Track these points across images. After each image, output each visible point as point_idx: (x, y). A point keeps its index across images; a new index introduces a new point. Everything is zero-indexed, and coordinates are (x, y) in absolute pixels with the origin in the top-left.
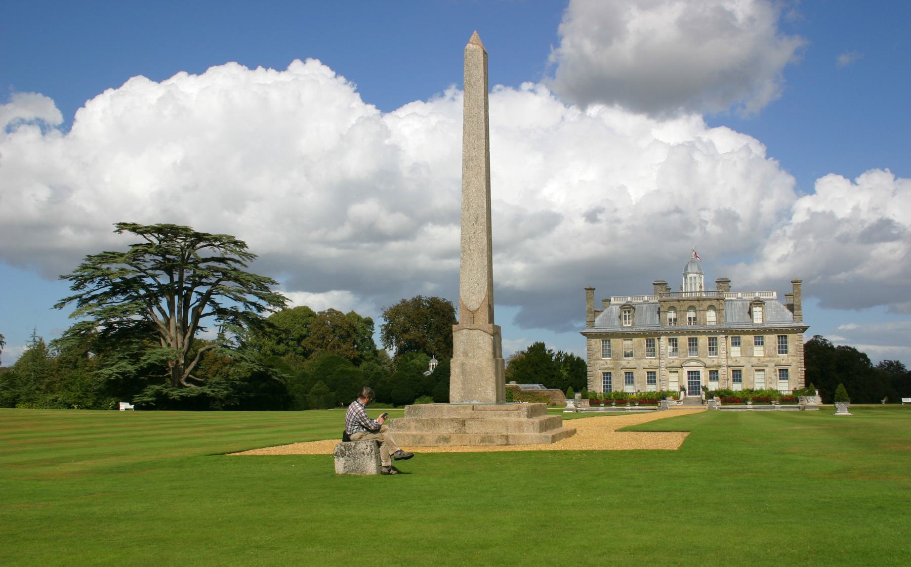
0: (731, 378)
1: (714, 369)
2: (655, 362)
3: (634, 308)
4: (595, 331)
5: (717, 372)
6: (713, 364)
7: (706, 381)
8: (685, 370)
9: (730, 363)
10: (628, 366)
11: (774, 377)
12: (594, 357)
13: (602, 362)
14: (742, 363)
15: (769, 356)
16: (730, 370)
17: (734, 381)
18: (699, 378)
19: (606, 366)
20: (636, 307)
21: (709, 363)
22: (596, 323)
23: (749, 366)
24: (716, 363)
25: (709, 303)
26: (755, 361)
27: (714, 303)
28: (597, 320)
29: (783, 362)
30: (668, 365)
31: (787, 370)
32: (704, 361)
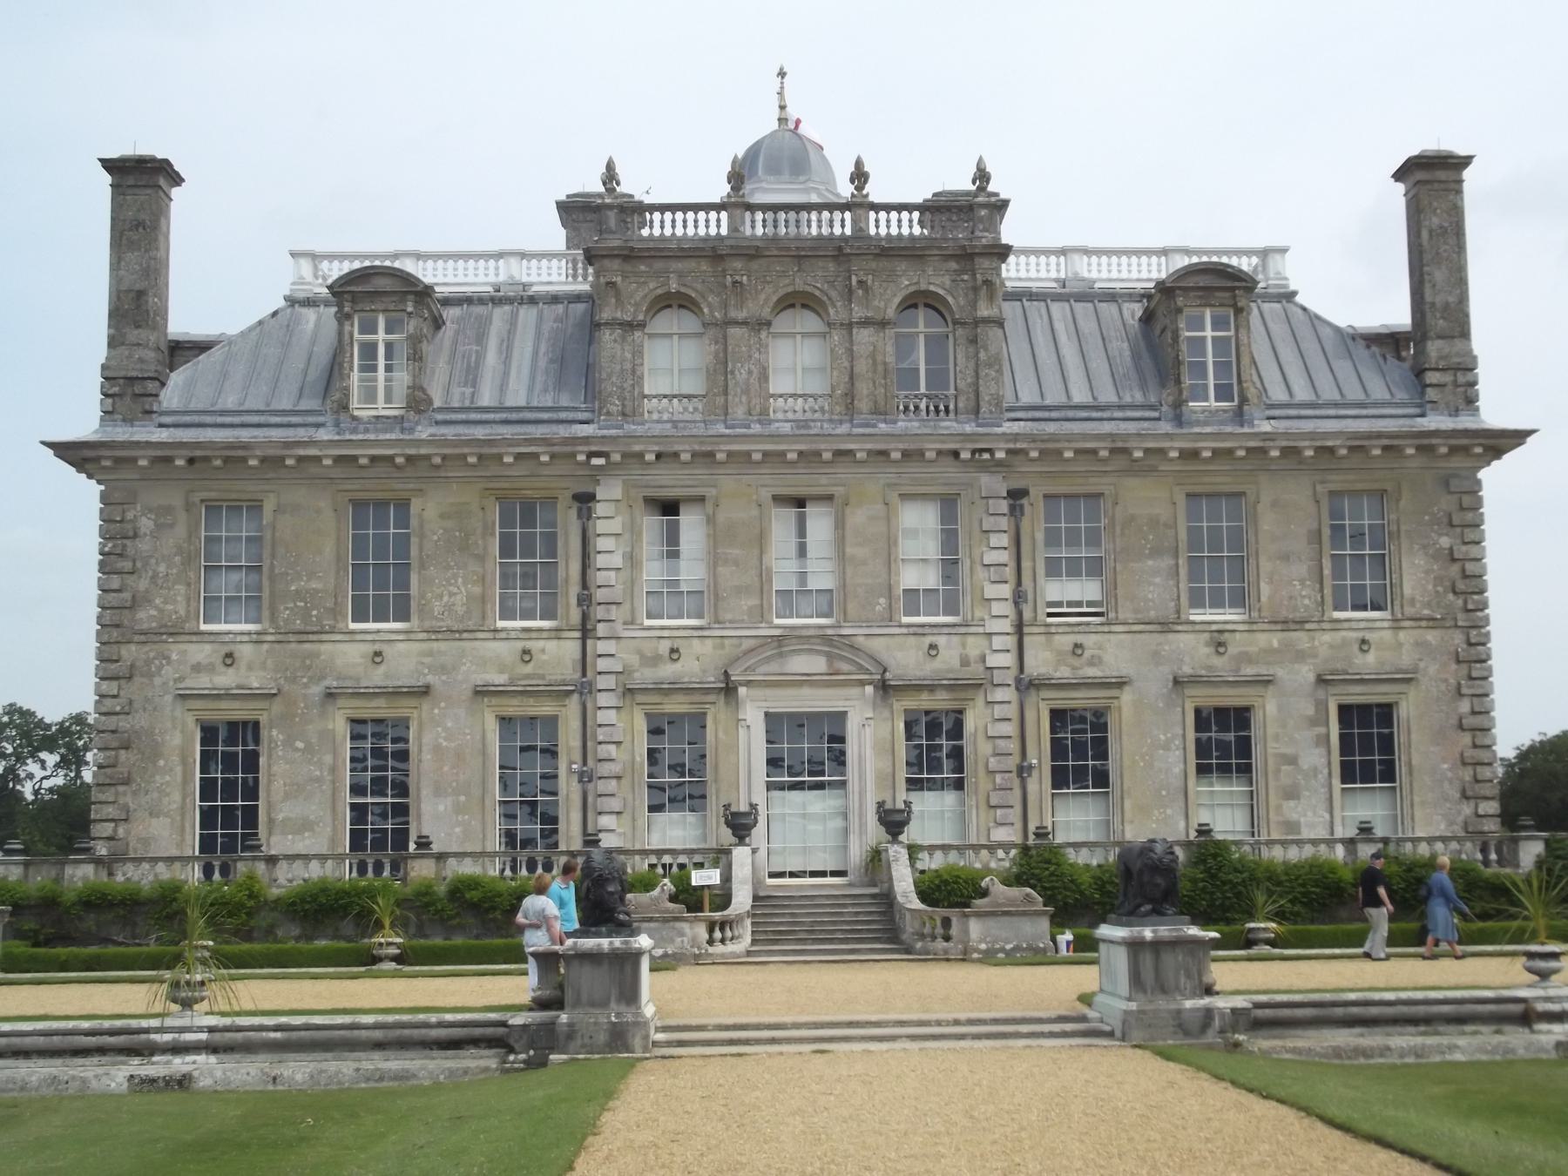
0: (1040, 755)
1: (940, 701)
8: (753, 715)
9: (1040, 661)
10: (377, 677)
12: (146, 617)
13: (201, 653)
15: (1287, 624)
17: (1060, 778)
19: (226, 679)
20: (450, 313)
21: (906, 660)
23: (1153, 683)
24: (949, 657)
25: (908, 280)
26: (1190, 650)
27: (937, 281)
28: (177, 378)
29: (1369, 662)
30: (645, 676)
31: (1386, 713)
32: (876, 646)
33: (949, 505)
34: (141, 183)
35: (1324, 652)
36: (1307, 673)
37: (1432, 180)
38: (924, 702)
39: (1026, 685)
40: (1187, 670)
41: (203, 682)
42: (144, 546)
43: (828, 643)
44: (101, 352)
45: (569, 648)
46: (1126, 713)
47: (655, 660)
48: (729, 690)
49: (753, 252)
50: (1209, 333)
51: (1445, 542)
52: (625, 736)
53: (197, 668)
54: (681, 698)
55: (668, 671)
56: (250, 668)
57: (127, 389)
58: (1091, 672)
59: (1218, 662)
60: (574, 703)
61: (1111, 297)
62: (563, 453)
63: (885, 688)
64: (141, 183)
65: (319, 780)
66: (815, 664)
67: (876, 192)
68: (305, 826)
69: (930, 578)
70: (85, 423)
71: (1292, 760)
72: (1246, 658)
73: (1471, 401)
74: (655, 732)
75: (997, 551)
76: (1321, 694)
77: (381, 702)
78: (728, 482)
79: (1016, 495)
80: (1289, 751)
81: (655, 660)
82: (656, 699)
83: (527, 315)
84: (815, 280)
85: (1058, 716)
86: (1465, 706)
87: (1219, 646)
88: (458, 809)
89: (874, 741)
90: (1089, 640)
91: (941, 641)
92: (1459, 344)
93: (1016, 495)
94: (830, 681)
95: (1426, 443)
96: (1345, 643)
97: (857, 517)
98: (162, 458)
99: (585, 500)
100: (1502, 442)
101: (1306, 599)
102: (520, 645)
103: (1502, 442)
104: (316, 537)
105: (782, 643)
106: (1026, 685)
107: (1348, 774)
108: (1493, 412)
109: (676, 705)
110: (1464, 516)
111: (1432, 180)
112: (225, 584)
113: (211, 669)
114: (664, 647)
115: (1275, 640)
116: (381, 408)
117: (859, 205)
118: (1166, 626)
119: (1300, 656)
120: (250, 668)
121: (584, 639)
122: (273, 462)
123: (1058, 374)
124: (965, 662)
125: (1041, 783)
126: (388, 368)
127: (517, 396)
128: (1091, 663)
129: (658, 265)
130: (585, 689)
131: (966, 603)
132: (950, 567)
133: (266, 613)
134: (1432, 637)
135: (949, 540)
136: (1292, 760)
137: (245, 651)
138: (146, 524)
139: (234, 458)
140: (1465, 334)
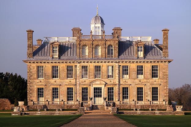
1: (111, 86)
2: (73, 81)
5: (113, 88)
13: (38, 81)
14: (129, 83)
19: (40, 84)
24: (112, 82)
34: (30, 32)
35: (151, 82)
36: (149, 84)
37: (165, 31)
38: (109, 86)
39: (119, 85)
40: (136, 84)
42: (32, 70)
45: (75, 81)
47: (83, 82)
50: (140, 49)
51: (164, 71)
52: (79, 89)
53: (37, 83)
54: (85, 86)
55: (84, 83)
56: (43, 82)
58: (127, 84)
59: (140, 83)
60: (75, 86)
65: (50, 94)
67: (106, 34)
69: (111, 74)
71: (147, 93)
72: (143, 83)
76: (151, 86)
77: (56, 86)
80: (147, 92)
81: (83, 82)
82: (83, 86)
86: (165, 88)
87: (140, 81)
88: (63, 97)
90: (126, 80)
91: (112, 80)
92: (167, 50)
94: (100, 84)
96: (153, 81)
102: (69, 80)
108: (170, 58)
109: (85, 87)
111: (165, 31)
113: (39, 83)
114: (84, 81)
115: (146, 80)
118: (134, 79)
119: (148, 82)
120: (43, 82)
121: (76, 80)
124: (114, 83)
126: (56, 52)
128: (127, 83)
129: (83, 42)
130: (76, 85)
131: (114, 77)
133: (44, 77)
134: (162, 80)
136: (147, 93)
137: (42, 81)
138: (32, 68)
140: (167, 49)
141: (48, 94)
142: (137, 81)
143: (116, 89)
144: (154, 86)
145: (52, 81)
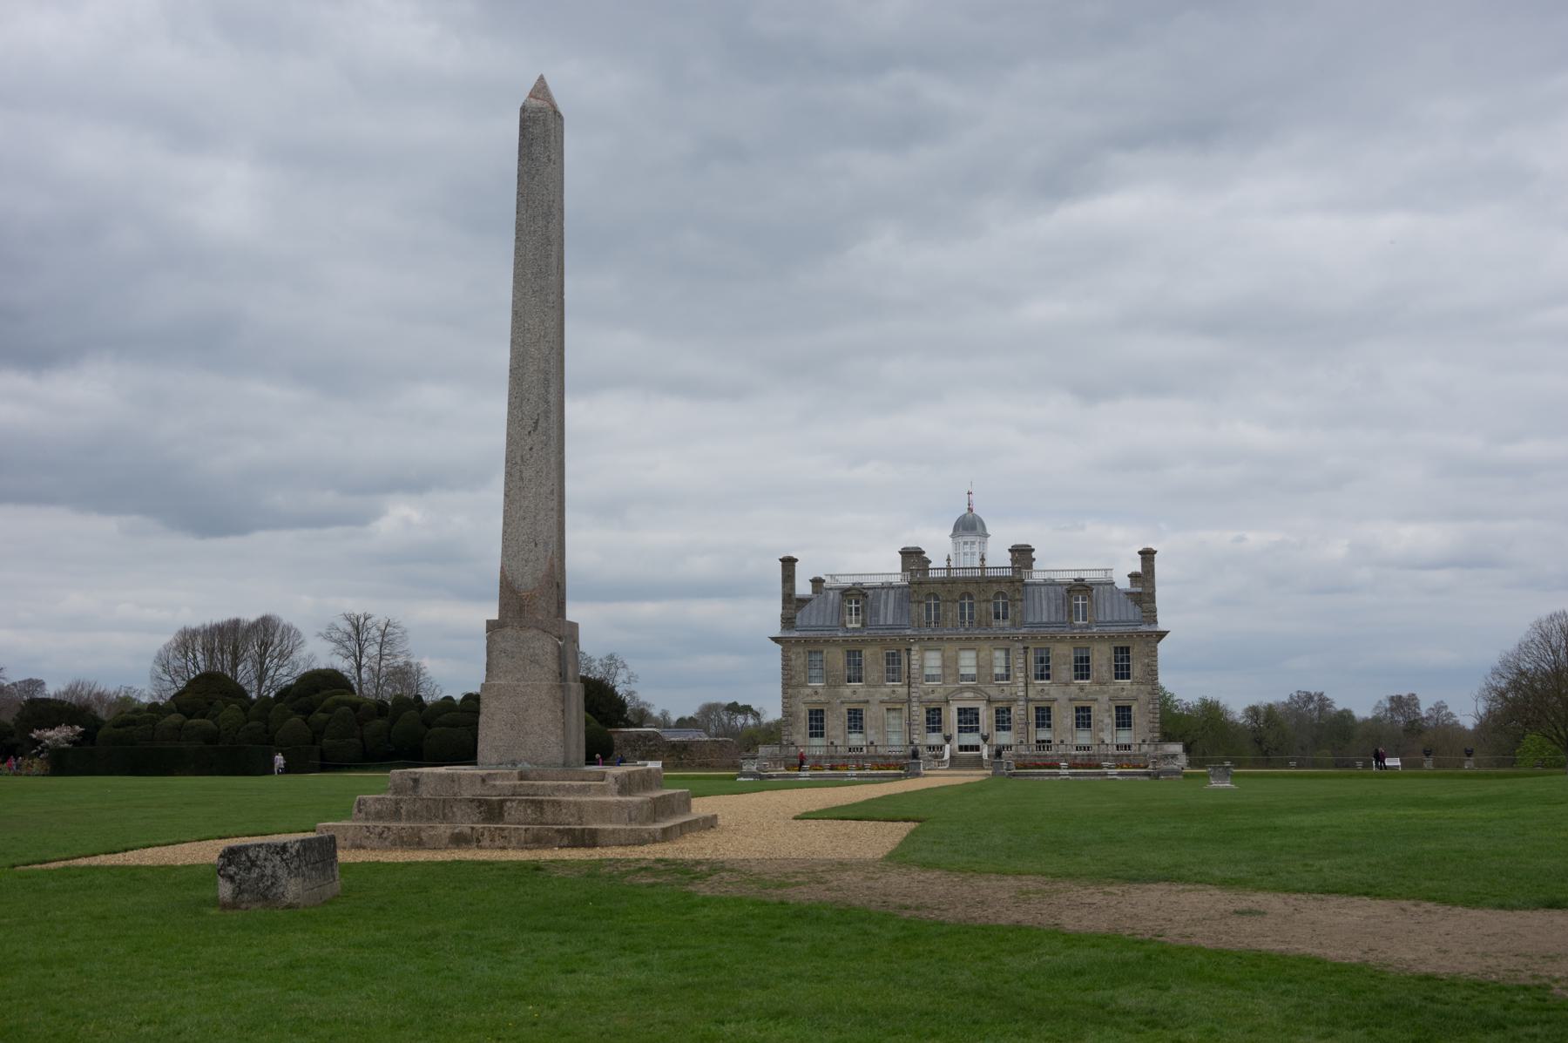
1: (1004, 705)
3: (865, 595)
4: (796, 634)
5: (1009, 710)
6: (1001, 697)
7: (989, 726)
9: (1031, 694)
10: (855, 698)
11: (1107, 720)
12: (794, 682)
15: (1101, 684)
16: (1032, 707)
17: (1038, 726)
18: (977, 720)
19: (815, 698)
20: (870, 592)
21: (994, 692)
22: (798, 622)
25: (996, 588)
26: (1073, 690)
30: (925, 698)
31: (1129, 708)
33: (1007, 651)
34: (789, 563)
36: (1106, 697)
37: (1147, 555)
38: (1000, 705)
39: (1028, 700)
41: (809, 699)
43: (973, 689)
44: (780, 610)
45: (905, 690)
46: (1055, 708)
48: (947, 702)
49: (954, 581)
55: (931, 696)
57: (788, 621)
60: (905, 708)
61: (1060, 584)
62: (903, 638)
63: (989, 701)
64: (789, 563)
66: (970, 695)
68: (837, 737)
69: (1003, 671)
70: (777, 632)
73: (1155, 622)
74: (928, 712)
75: (1020, 663)
78: (947, 645)
79: (1026, 648)
83: (892, 592)
84: (971, 588)
85: (1037, 709)
89: (986, 717)
93: (1026, 648)
95: (1139, 634)
97: (982, 654)
98: (798, 641)
99: (909, 650)
100: (1162, 635)
101: (1106, 676)
103: (1162, 635)
104: (837, 659)
105: (961, 690)
106: (1028, 700)
107: (1118, 725)
108: (1161, 627)
110: (1153, 654)
111: (1147, 555)
112: (814, 672)
116: (854, 625)
117: (983, 568)
118: (1067, 684)
122: (827, 641)
123: (1043, 611)
125: (1032, 727)
127: (890, 621)
130: (909, 701)
132: (1008, 668)
135: (1007, 659)
139: (816, 641)
141: (835, 724)
142: (1073, 690)
143: (1017, 711)
144: (1120, 703)
145: (847, 691)
